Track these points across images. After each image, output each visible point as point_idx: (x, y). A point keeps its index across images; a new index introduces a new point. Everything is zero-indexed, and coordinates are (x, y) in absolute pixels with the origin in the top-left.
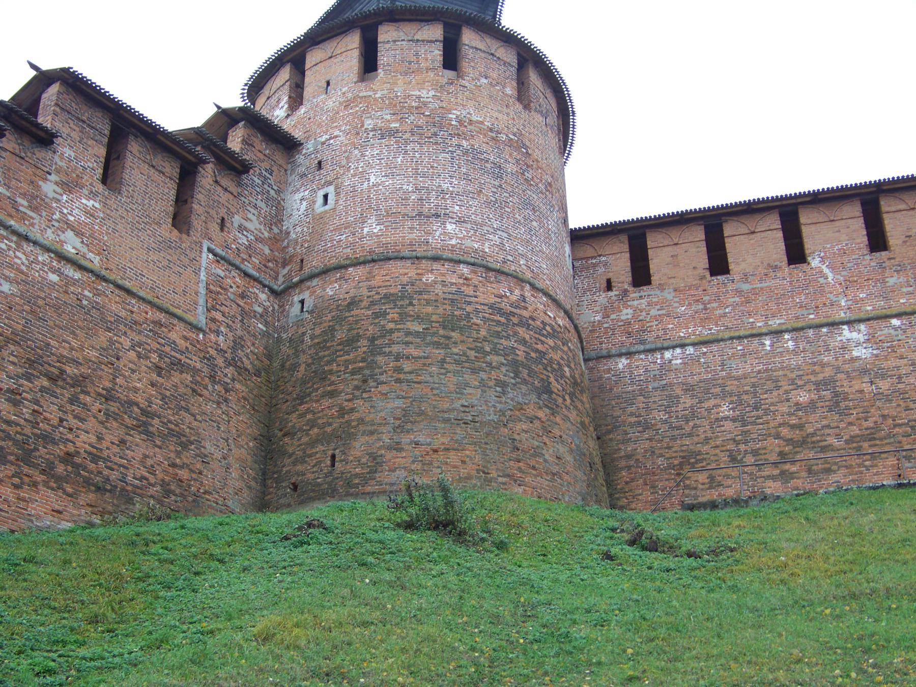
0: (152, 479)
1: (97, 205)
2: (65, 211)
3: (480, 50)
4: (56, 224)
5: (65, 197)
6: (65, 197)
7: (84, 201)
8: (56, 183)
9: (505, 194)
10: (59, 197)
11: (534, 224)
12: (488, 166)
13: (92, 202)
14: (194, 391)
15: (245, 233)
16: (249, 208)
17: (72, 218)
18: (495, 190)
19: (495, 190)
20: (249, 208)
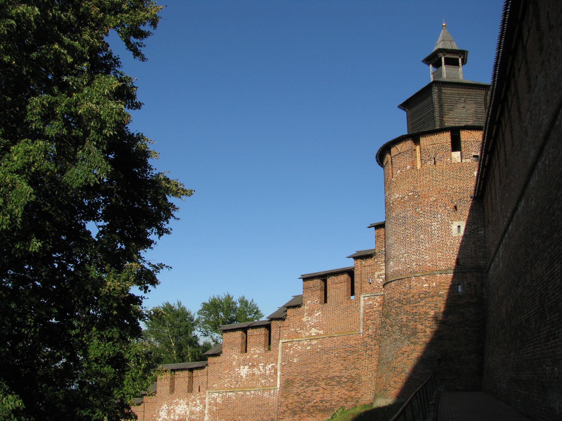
0: (341, 400)
1: (320, 313)
2: (310, 323)
3: (396, 155)
4: (308, 329)
5: (310, 318)
6: (310, 318)
7: (316, 315)
8: (307, 316)
9: (407, 231)
10: (308, 320)
11: (422, 236)
12: (401, 221)
13: (318, 313)
14: (358, 358)
15: (381, 277)
16: (381, 265)
17: (313, 324)
18: (403, 232)
19: (403, 232)
20: (381, 265)
